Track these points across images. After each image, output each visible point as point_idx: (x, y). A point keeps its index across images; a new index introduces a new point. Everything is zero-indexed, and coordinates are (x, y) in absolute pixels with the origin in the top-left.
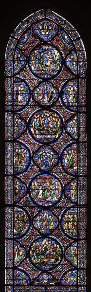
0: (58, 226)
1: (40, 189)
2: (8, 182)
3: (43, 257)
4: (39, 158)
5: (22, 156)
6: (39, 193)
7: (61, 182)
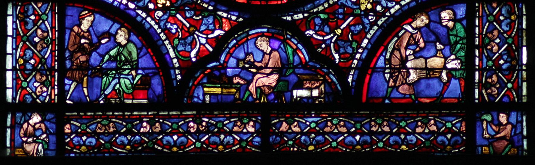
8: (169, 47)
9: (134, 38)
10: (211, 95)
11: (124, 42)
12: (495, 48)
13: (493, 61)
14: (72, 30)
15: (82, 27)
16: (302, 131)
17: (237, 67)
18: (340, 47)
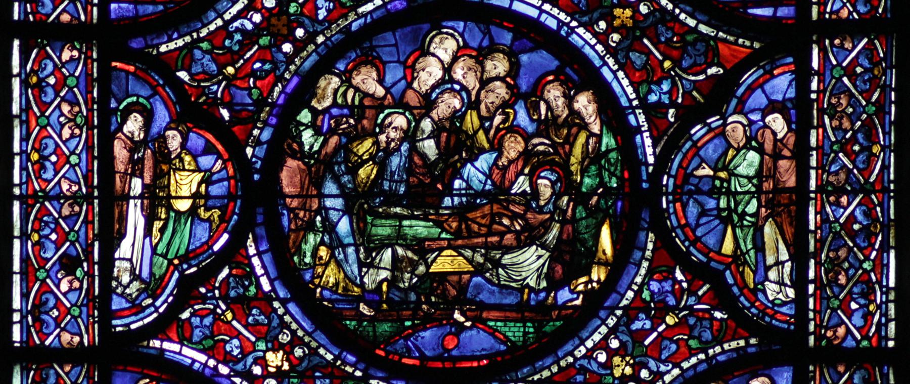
3: (420, 228)
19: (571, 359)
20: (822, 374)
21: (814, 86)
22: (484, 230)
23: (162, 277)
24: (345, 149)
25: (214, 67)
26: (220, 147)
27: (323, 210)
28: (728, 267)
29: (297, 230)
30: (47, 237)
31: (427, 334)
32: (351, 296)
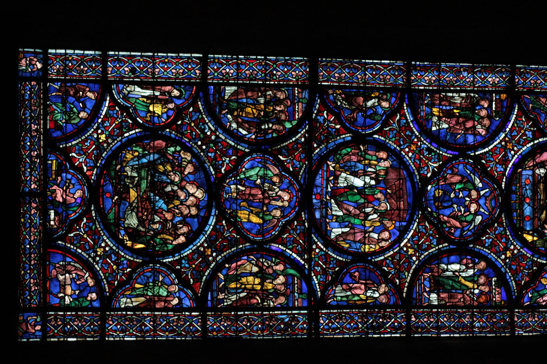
0: (248, 240)
1: (367, 179)
2: (383, 70)
3: (144, 185)
4: (463, 177)
5: (467, 119)
6: (355, 174)
7: (388, 249)
8: (78, 141)
9: (83, 122)
10: (52, 164)
11: (80, 116)
12: (76, 323)
13: (69, 322)
14: (87, 87)
15: (89, 93)
16: (32, 215)
17: (67, 179)
18: (77, 236)
19: (102, 234)
20: (97, 316)
21: (187, 313)
22: (143, 206)
23: (129, 101)
24: (168, 161)
25: (194, 119)
26: (169, 121)
27: (150, 154)
28: (131, 286)
29: (144, 146)
30: (142, 64)
31: (110, 187)
32: (123, 162)
